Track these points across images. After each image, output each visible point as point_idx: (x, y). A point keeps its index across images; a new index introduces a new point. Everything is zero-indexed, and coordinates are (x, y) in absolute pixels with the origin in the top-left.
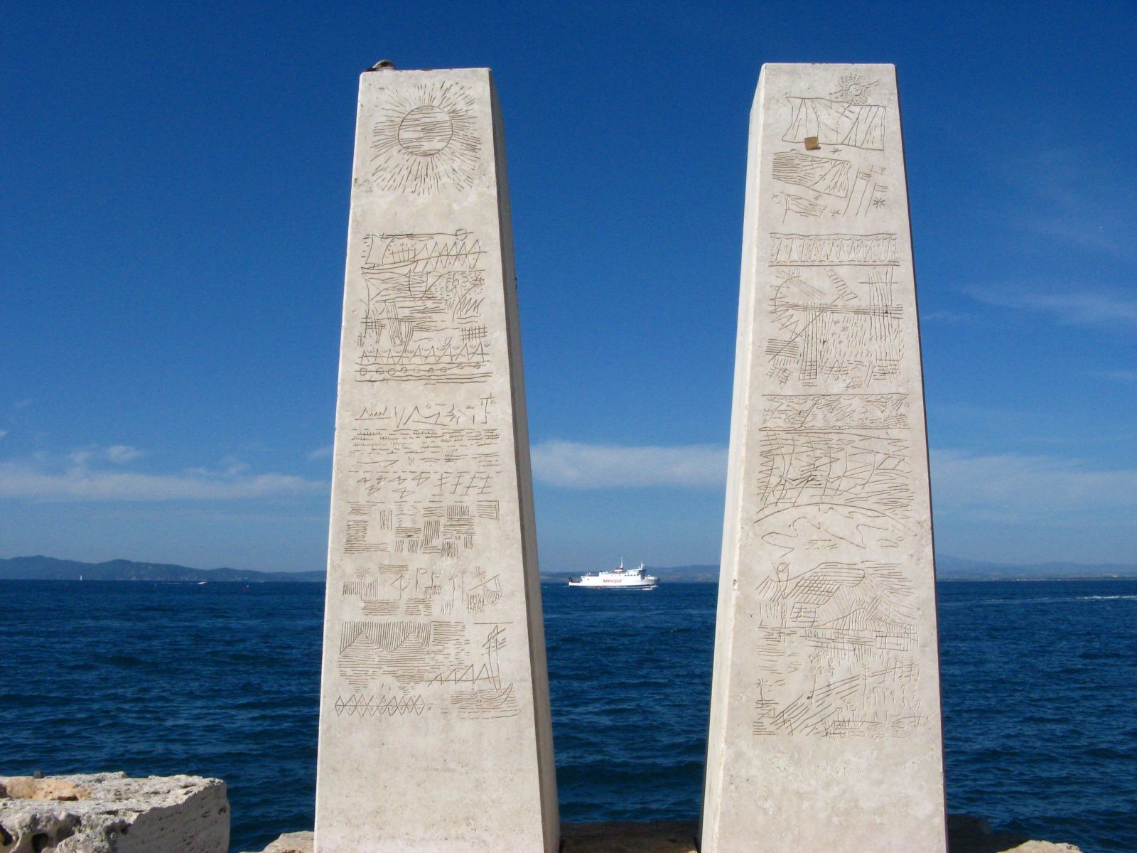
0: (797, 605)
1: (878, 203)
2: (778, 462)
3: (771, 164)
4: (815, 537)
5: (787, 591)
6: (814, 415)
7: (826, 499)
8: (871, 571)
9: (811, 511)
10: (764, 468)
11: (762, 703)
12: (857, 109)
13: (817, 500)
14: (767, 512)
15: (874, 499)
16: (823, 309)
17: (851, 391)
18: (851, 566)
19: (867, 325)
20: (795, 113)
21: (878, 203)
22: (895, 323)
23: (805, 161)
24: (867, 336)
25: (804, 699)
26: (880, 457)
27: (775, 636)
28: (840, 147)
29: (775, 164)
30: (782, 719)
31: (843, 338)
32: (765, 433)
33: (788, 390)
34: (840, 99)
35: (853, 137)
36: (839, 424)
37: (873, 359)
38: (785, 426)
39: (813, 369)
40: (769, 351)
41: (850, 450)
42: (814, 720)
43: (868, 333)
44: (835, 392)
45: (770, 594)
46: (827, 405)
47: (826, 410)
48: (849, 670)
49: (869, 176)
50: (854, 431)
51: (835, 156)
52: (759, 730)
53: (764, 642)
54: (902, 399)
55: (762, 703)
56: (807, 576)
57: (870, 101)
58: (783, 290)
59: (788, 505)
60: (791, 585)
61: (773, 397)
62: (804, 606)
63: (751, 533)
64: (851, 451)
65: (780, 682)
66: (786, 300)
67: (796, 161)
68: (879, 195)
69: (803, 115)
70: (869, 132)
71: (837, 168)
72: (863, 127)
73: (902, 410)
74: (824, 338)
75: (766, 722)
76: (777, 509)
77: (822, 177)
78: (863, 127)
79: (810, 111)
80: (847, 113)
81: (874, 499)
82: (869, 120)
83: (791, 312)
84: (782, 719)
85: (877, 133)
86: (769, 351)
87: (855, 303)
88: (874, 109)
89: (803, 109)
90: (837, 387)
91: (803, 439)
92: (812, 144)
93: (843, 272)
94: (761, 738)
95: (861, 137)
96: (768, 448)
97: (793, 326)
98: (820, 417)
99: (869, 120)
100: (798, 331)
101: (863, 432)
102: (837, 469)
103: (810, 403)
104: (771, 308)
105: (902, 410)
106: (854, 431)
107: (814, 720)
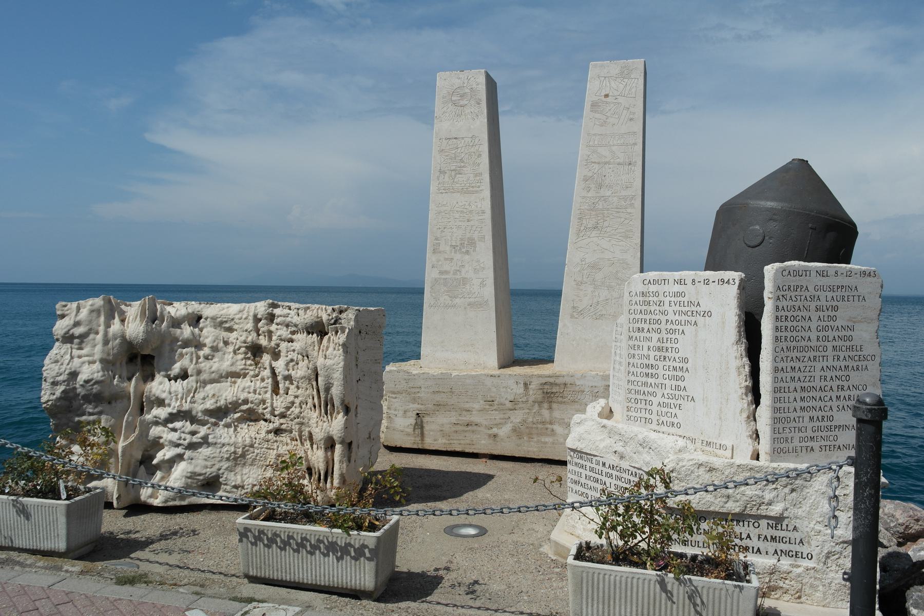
1: (631, 119)
2: (584, 221)
7: (601, 235)
9: (595, 239)
12: (626, 80)
13: (598, 235)
14: (579, 239)
16: (606, 163)
17: (613, 195)
18: (609, 260)
21: (631, 119)
26: (622, 220)
28: (618, 97)
29: (591, 105)
30: (581, 313)
33: (590, 195)
39: (600, 186)
41: (611, 217)
42: (592, 314)
45: (579, 269)
51: (616, 101)
52: (572, 316)
54: (633, 197)
55: (574, 307)
57: (632, 76)
61: (584, 197)
64: (611, 217)
68: (631, 116)
69: (604, 85)
70: (630, 89)
72: (628, 88)
75: (575, 314)
78: (628, 88)
79: (608, 82)
84: (581, 313)
85: (633, 90)
86: (584, 180)
87: (618, 160)
88: (633, 80)
90: (608, 193)
91: (594, 213)
92: (607, 96)
93: (614, 148)
98: (601, 205)
101: (617, 210)
102: (606, 224)
103: (598, 200)
107: (592, 314)
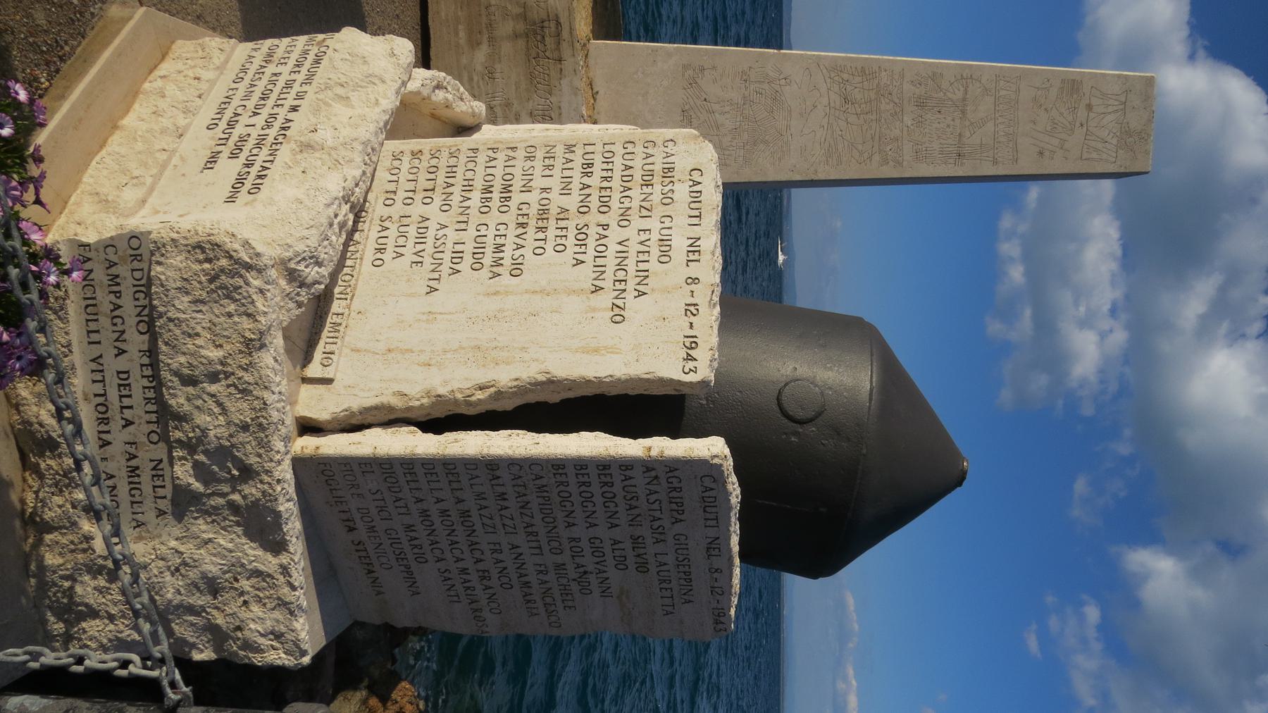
0: (764, 92)
1: (1041, 153)
2: (858, 79)
3: (1074, 78)
4: (808, 103)
5: (773, 85)
6: (889, 104)
7: (832, 110)
8: (785, 139)
9: (825, 101)
10: (854, 70)
11: (703, 69)
12: (1114, 141)
13: (832, 105)
14: (825, 71)
15: (832, 142)
16: (963, 112)
17: (905, 129)
18: (788, 127)
19: (950, 141)
20: (1114, 97)
21: (1041, 153)
22: (952, 161)
23: (1075, 102)
24: (942, 141)
25: (705, 96)
26: (860, 147)
27: (745, 78)
28: (1085, 129)
29: (1074, 80)
30: (693, 83)
31: (942, 125)
32: (877, 70)
33: (907, 86)
34: (1123, 130)
35: (1093, 138)
36: (883, 120)
37: (927, 145)
38: (882, 84)
39: (921, 103)
40: (934, 74)
41: (865, 128)
42: (692, 103)
43: (945, 142)
44: (905, 118)
45: (771, 74)
46: (896, 113)
47: (893, 111)
48: (723, 125)
49: (1062, 148)
50: (878, 130)
51: (1078, 124)
52: (686, 67)
53: (741, 70)
54: (899, 163)
55: (703, 69)
56: (783, 98)
57: (1121, 151)
58: (978, 84)
59: (829, 85)
60: (777, 88)
61: (902, 76)
62: (764, 96)
63: (810, 61)
64: (865, 128)
65: (715, 81)
66: (971, 85)
67: (1075, 96)
68: (1047, 153)
69: (1111, 102)
70: (1096, 150)
71: (1068, 125)
72: (1100, 146)
73: (891, 163)
74: (943, 111)
75: (690, 72)
76: (827, 78)
77: (1062, 114)
78: (1100, 146)
79: (1115, 108)
80: (1112, 134)
81: (832, 142)
82: (1104, 150)
83: (962, 89)
84: (693, 83)
85: (1094, 155)
86: (934, 74)
87: (968, 134)
88: (1115, 155)
89: (1116, 103)
90: (908, 120)
91: (873, 95)
92: (1089, 107)
93: (990, 125)
94: (680, 69)
95: (1093, 144)
96: (867, 72)
97: (951, 90)
98: (888, 107)
99: (1104, 150)
100: (948, 94)
101: (877, 137)
102: (852, 119)
103: (897, 101)
104: (965, 76)
105: (891, 163)
106: (878, 130)
107: (692, 103)
